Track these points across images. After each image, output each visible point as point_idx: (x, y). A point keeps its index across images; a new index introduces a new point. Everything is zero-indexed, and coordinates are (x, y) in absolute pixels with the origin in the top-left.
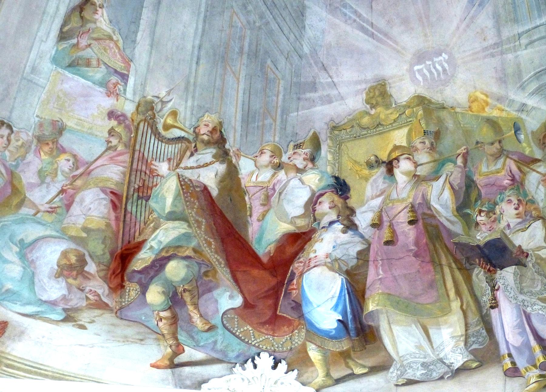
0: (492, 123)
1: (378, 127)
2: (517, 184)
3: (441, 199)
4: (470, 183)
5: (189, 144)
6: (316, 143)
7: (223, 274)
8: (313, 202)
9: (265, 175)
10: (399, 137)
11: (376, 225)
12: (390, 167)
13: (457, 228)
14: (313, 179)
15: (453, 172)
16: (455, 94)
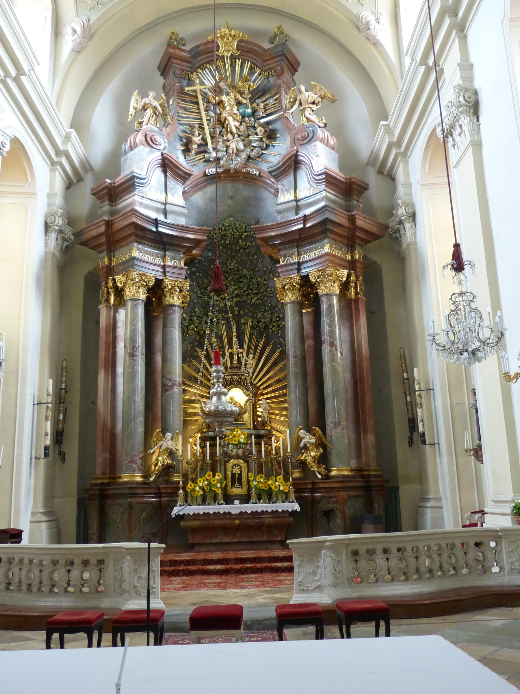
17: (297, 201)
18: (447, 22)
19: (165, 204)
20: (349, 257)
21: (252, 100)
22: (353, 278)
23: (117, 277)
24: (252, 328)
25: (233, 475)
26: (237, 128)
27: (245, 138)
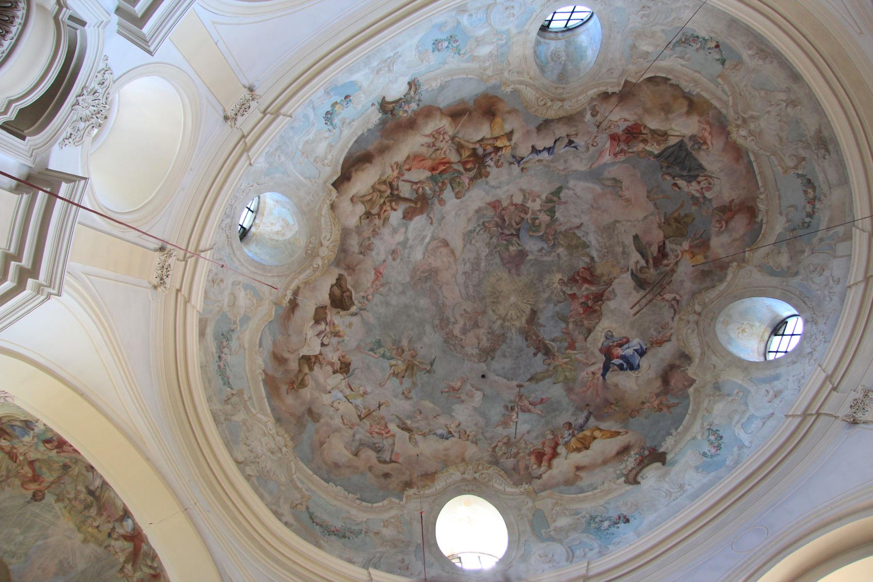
0: (69, 513)
1: (92, 536)
2: (76, 499)
3: (93, 511)
4: (85, 508)
5: (126, 576)
6: (106, 547)
7: (142, 551)
8: (117, 539)
9: (120, 554)
10: (90, 529)
11: (109, 522)
12: (98, 527)
13: (95, 504)
14: (113, 543)
15: (86, 513)
16: (71, 525)
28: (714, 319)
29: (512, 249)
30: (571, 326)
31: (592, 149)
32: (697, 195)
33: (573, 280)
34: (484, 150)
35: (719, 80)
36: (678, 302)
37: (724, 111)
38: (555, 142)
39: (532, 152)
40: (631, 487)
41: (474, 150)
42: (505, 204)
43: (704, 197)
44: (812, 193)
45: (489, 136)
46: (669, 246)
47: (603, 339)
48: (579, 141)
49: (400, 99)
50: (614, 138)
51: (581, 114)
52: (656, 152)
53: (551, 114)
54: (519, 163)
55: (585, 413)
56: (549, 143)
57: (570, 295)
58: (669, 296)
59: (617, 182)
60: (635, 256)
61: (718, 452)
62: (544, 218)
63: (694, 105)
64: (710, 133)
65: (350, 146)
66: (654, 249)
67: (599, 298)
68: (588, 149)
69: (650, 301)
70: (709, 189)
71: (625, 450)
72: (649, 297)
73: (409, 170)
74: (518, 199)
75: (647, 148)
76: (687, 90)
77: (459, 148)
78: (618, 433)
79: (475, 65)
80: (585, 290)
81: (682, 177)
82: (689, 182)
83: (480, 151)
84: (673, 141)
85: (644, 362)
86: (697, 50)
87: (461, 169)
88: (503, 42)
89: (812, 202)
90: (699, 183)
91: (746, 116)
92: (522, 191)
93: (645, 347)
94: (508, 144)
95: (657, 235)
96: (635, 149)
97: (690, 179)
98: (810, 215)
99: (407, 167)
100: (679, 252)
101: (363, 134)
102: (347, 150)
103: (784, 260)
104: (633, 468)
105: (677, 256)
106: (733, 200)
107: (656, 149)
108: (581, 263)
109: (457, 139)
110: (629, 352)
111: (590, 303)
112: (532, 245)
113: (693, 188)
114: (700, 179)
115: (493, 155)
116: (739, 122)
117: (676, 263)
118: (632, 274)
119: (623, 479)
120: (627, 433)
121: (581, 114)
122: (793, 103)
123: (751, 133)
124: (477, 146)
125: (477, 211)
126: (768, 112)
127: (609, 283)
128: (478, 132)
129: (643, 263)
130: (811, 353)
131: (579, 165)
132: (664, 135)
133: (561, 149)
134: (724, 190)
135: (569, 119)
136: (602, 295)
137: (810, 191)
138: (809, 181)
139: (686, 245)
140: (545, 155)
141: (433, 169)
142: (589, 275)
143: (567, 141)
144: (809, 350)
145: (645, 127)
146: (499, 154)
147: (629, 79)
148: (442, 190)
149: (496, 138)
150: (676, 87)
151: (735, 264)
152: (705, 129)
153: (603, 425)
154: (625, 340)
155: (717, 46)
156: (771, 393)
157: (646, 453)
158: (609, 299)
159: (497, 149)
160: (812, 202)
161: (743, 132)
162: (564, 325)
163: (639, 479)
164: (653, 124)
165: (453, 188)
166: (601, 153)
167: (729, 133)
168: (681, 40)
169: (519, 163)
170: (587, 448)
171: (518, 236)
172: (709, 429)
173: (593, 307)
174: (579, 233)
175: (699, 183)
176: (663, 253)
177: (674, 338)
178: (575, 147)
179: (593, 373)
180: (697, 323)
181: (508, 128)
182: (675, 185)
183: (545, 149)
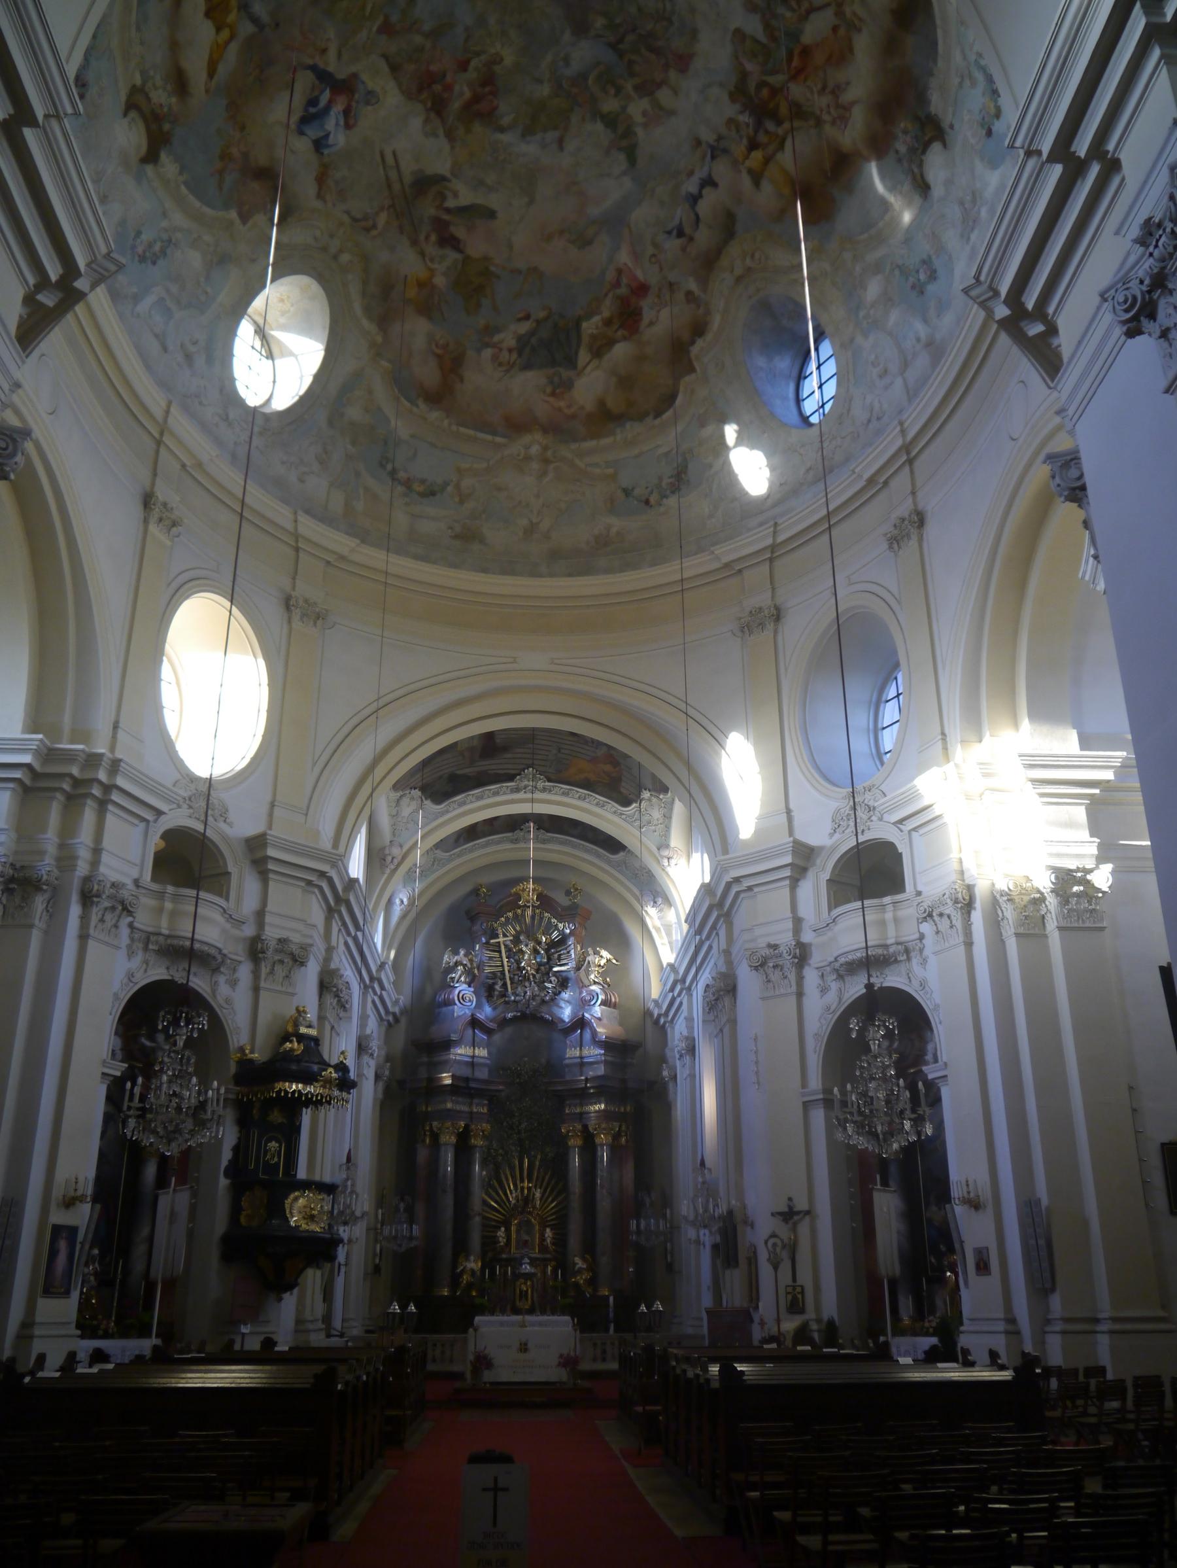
17: (581, 1058)
18: (678, 988)
19: (473, 1057)
20: (622, 1109)
21: (547, 951)
22: (624, 1128)
23: (435, 1124)
24: (541, 1160)
25: (521, 1291)
26: (534, 976)
27: (541, 985)
28: (321, 279)
29: (599, 22)
30: (418, 39)
31: (650, 250)
32: (496, 338)
33: (488, 81)
34: (767, 132)
35: (610, 471)
36: (368, 230)
37: (574, 446)
38: (697, 216)
39: (710, 175)
40: (123, 98)
41: (779, 123)
42: (673, 74)
43: (487, 345)
44: (418, 489)
45: (779, 156)
46: (452, 256)
47: (371, 85)
48: (673, 245)
49: (924, 152)
50: (642, 289)
51: (704, 282)
52: (584, 325)
53: (734, 250)
54: (713, 148)
55: (265, 18)
56: (703, 207)
57: (468, 62)
58: (382, 218)
59: (584, 242)
60: (465, 196)
61: (137, 258)
62: (610, 105)
63: (605, 418)
64: (560, 409)
65: (939, 32)
66: (459, 232)
67: (438, 107)
68: (655, 245)
69: (389, 186)
70: (495, 358)
71: (180, 84)
72: (397, 187)
73: (835, 29)
74: (664, 95)
75: (596, 319)
76: (628, 425)
77: (799, 112)
78: (211, 73)
79: (872, 257)
80: (462, 91)
81: (532, 333)
82: (520, 338)
83: (770, 125)
84: (583, 356)
85: (302, 145)
86: (660, 479)
87: (771, 79)
88: (862, 314)
89: (407, 484)
90: (510, 351)
91: (552, 466)
92: (671, 113)
93: (326, 151)
94: (748, 163)
95: (476, 246)
96: (608, 302)
97: (523, 342)
98: (393, 474)
99: (842, 32)
100: (436, 266)
101: (935, 61)
102: (938, 22)
103: (354, 413)
104: (149, 99)
105: (432, 260)
106: (462, 380)
107: (590, 327)
108: (506, 110)
109: (812, 122)
110: (332, 123)
111: (437, 88)
112: (584, 54)
113: (508, 338)
114: (514, 356)
115: (751, 131)
116: (549, 453)
117: (422, 254)
118: (443, 179)
119: (138, 81)
120: (207, 91)
121: (704, 282)
122: (530, 530)
123: (528, 458)
124: (780, 131)
125: (694, 34)
126: (538, 496)
127: (450, 136)
128: (796, 153)
129: (451, 203)
130: (226, 419)
131: (643, 215)
132: (600, 349)
133: (681, 213)
134: (482, 378)
135: (708, 263)
136: (439, 113)
137: (421, 489)
138: (433, 494)
139: (440, 281)
140: (691, 187)
141: (806, 52)
142: (480, 110)
143: (688, 230)
144: (231, 416)
145: (625, 338)
146: (745, 141)
147: (693, 376)
148: (767, 26)
149: (767, 161)
150: (641, 417)
151: (379, 339)
152: (569, 407)
153: (233, 48)
154: (351, 122)
155: (647, 502)
156: (192, 349)
157: (166, 127)
158: (427, 121)
159: (753, 146)
160: (407, 484)
161: (535, 449)
162: (427, 27)
163: (133, 114)
164: (621, 351)
165: (756, 41)
166: (636, 256)
167: (545, 431)
168: (685, 473)
169: (713, 148)
170: (207, 14)
171: (613, 46)
172: (170, 241)
173: (429, 91)
174: (551, 136)
175: (510, 351)
176: (448, 241)
177: (318, 204)
178: (669, 233)
179: (324, 51)
180: (324, 249)
181: (767, 187)
182: (527, 317)
183: (700, 196)
